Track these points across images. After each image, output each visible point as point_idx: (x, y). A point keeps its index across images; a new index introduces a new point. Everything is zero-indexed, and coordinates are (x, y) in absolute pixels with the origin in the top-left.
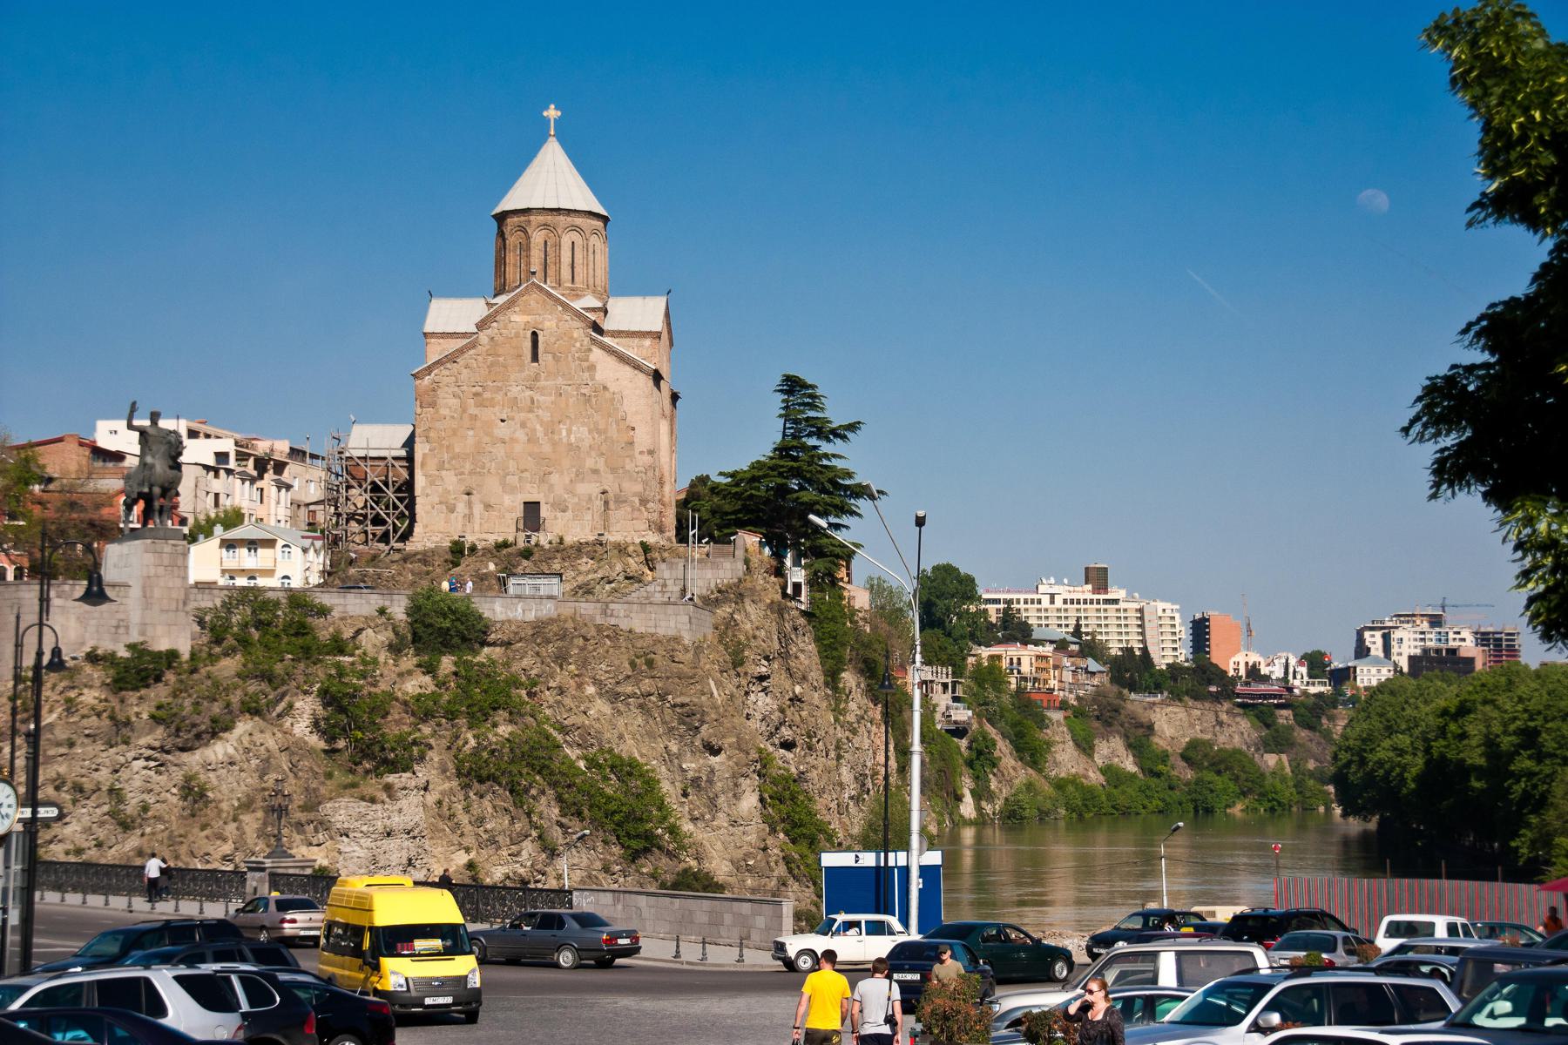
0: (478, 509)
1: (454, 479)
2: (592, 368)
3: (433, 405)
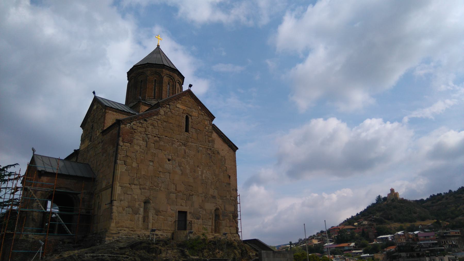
0: (151, 214)
1: (138, 191)
2: (213, 141)
3: (131, 142)
